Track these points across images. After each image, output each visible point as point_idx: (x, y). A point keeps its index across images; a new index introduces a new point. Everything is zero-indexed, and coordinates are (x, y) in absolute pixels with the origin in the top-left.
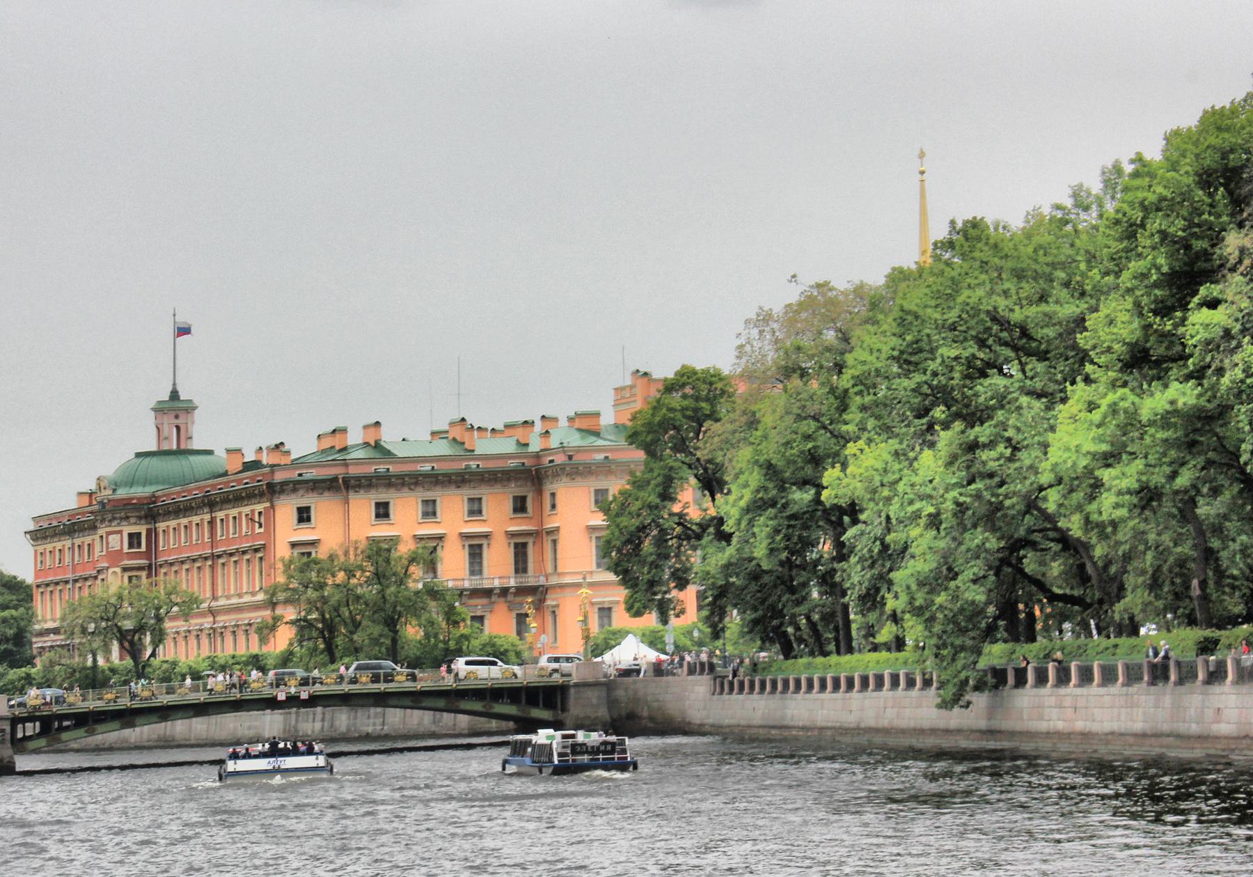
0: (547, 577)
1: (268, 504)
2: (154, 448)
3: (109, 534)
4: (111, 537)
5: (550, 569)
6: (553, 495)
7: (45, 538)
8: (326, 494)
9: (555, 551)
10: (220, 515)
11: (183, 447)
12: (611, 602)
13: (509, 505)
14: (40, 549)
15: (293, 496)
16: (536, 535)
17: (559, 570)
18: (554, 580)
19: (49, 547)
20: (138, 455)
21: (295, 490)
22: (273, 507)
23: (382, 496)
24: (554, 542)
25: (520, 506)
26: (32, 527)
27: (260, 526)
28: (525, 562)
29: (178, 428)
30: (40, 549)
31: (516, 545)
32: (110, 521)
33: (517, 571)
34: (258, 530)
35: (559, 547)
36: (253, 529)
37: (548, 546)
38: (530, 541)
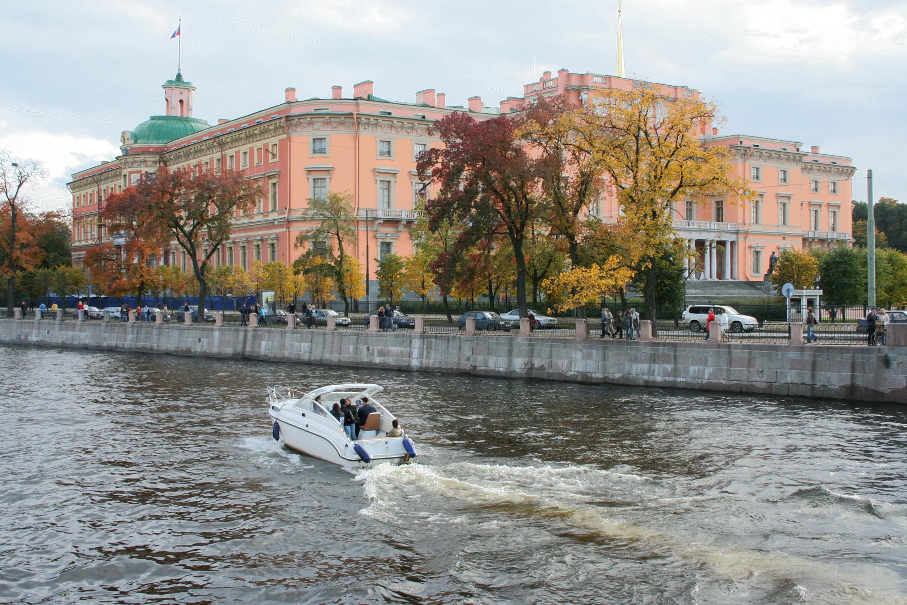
1: (285, 136)
2: (163, 113)
3: (130, 173)
4: (132, 176)
7: (80, 187)
8: (342, 128)
10: (229, 152)
11: (185, 116)
14: (77, 194)
15: (310, 129)
19: (83, 193)
20: (153, 118)
21: (311, 124)
22: (289, 138)
23: (386, 133)
26: (71, 180)
27: (274, 156)
29: (181, 101)
30: (77, 194)
32: (132, 163)
34: (271, 161)
36: (266, 159)
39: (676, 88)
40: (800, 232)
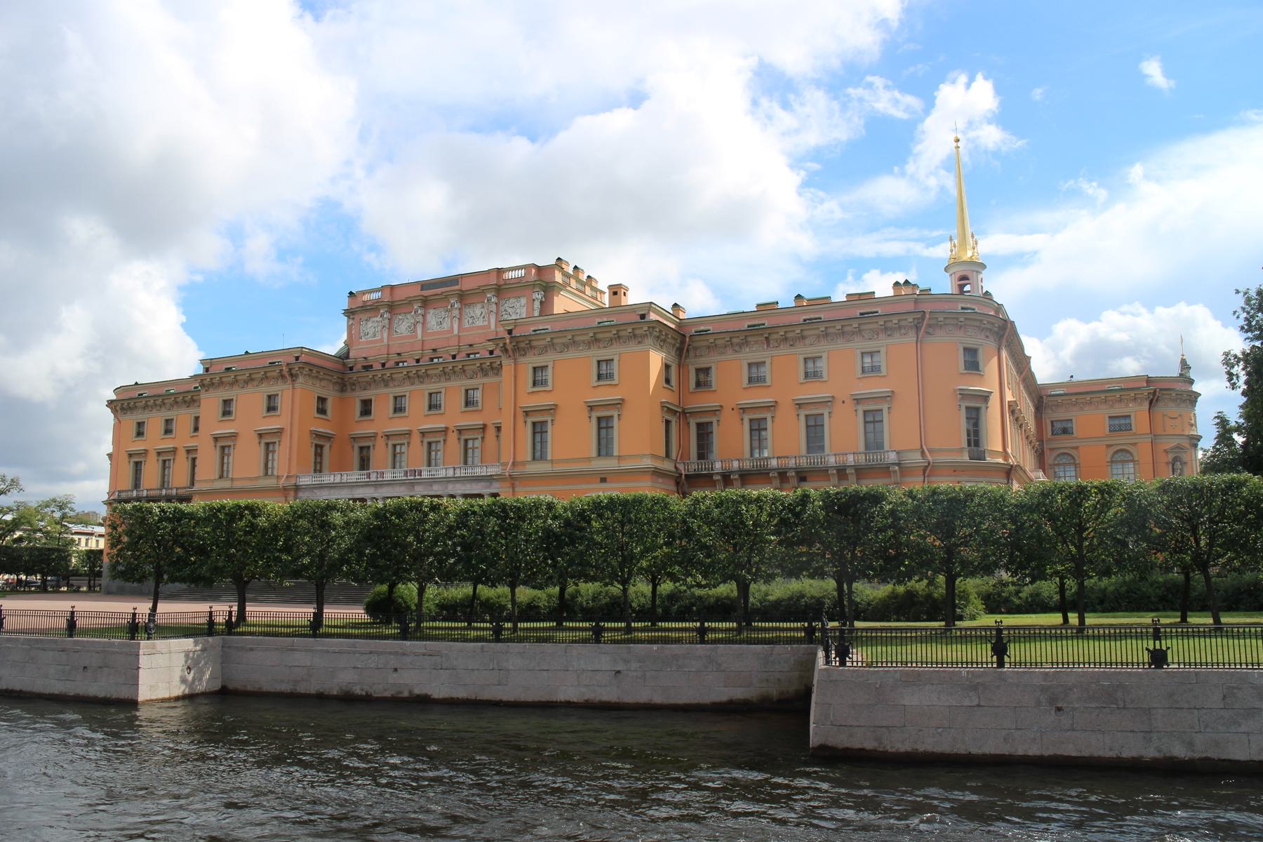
39: (489, 271)
40: (648, 463)
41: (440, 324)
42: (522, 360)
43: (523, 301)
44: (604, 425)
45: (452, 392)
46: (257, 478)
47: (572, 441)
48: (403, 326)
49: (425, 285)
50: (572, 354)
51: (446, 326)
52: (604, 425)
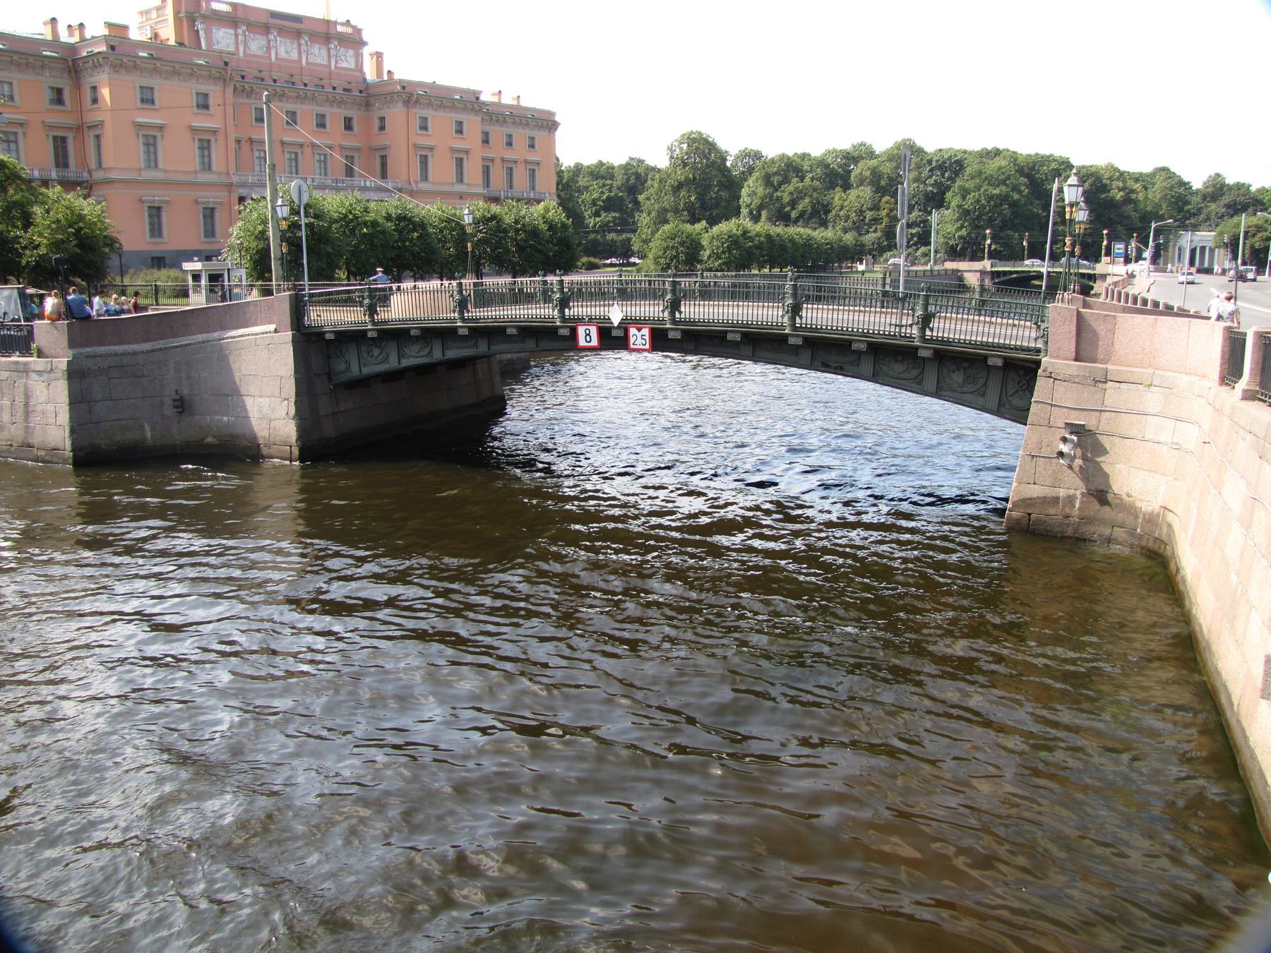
0: (90, 172)
5: (93, 165)
6: (94, 88)
9: (99, 146)
12: (160, 202)
13: (48, 95)
16: (79, 129)
17: (105, 165)
18: (99, 175)
24: (98, 137)
25: (58, 97)
28: (66, 156)
31: (55, 138)
33: (57, 165)
35: (103, 141)
37: (91, 142)
38: (71, 137)
40: (480, 190)
41: (285, 50)
42: (414, 110)
43: (351, 52)
44: (460, 162)
45: (307, 112)
46: (196, 172)
47: (441, 170)
48: (256, 45)
49: (274, 15)
50: (441, 114)
51: (294, 55)
52: (460, 162)
